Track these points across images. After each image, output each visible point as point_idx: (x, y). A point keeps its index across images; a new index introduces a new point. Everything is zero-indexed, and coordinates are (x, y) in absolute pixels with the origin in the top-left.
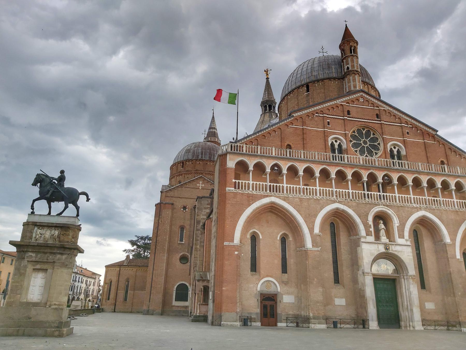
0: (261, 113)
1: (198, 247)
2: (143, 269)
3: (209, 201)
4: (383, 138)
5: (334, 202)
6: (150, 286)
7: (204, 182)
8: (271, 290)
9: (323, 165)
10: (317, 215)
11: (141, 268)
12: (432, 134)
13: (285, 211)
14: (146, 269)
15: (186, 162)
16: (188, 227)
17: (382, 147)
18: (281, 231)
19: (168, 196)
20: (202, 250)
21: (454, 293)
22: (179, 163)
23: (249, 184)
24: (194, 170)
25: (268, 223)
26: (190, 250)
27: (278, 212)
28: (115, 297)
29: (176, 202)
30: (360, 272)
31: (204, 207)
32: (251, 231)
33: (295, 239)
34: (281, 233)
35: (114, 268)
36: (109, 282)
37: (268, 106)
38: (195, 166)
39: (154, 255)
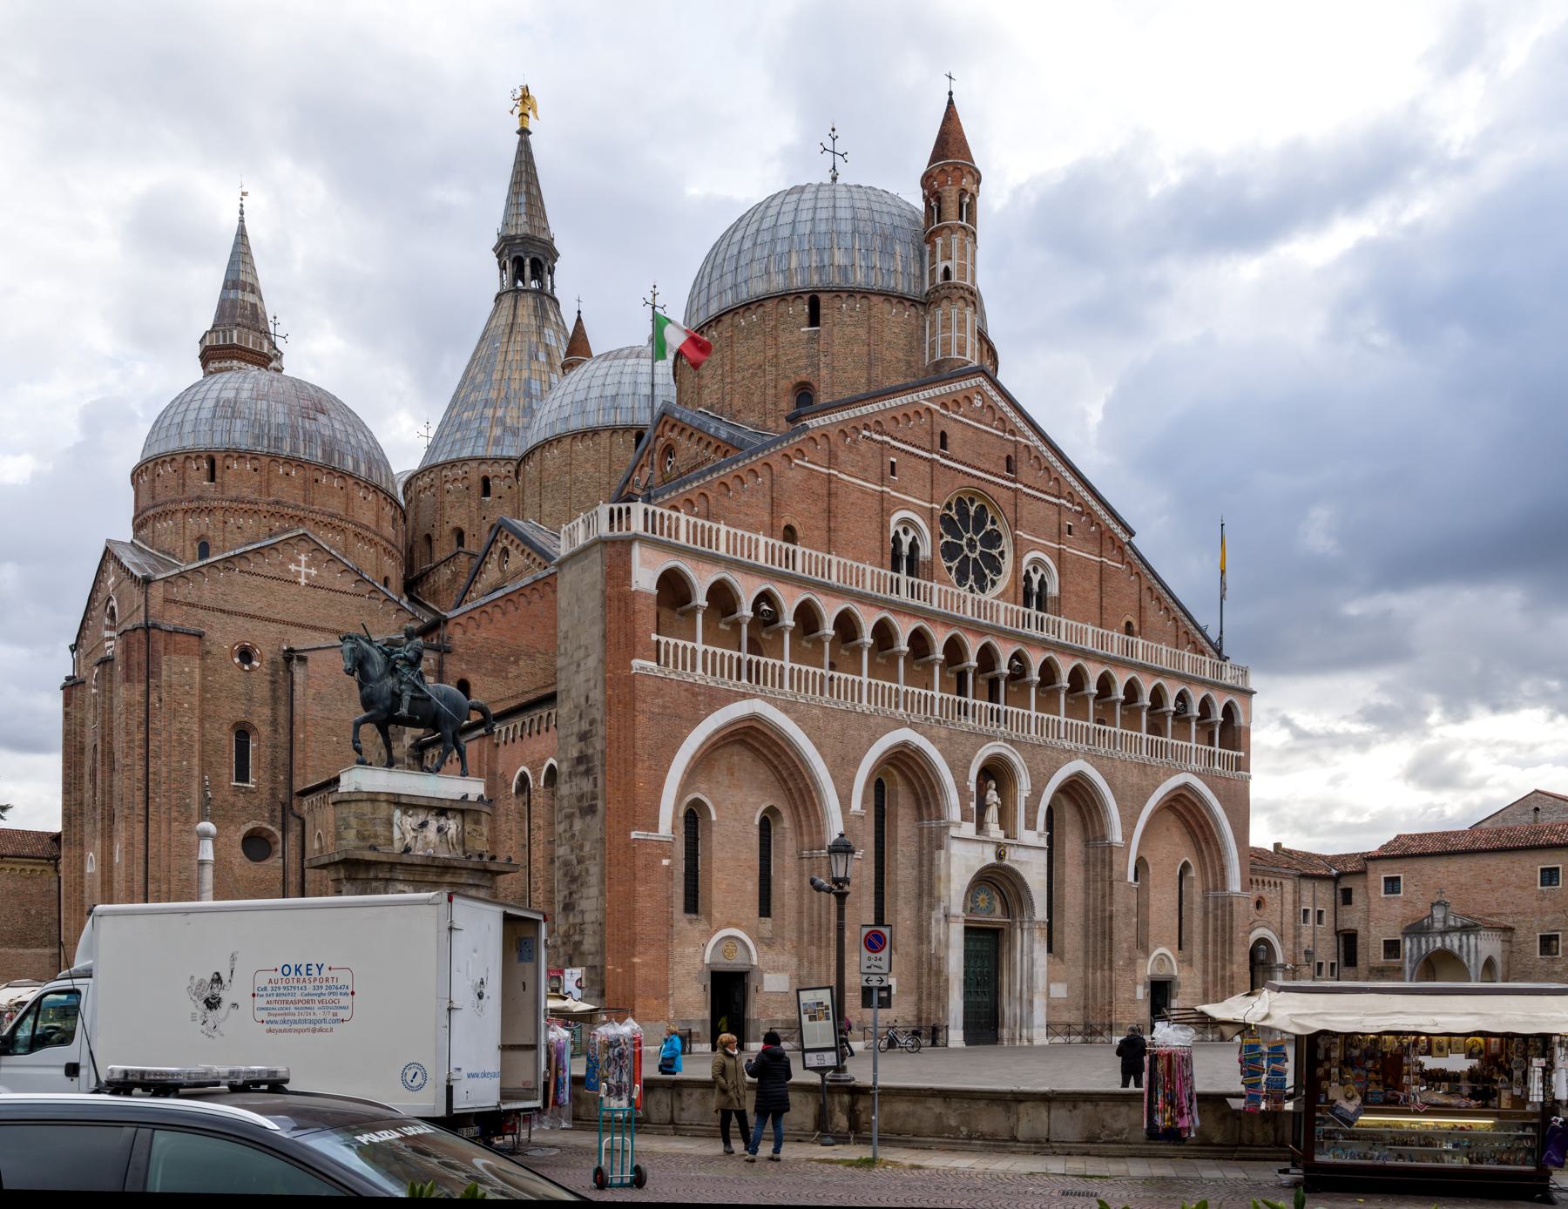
0: (497, 289)
4: (1015, 538)
5: (901, 724)
8: (736, 962)
9: (882, 608)
10: (860, 761)
12: (1120, 540)
13: (783, 745)
14: (31, 867)
17: (1007, 565)
18: (763, 801)
21: (1111, 962)
22: (188, 457)
23: (694, 650)
24: (265, 498)
25: (732, 774)
26: (279, 814)
27: (762, 743)
29: (211, 627)
30: (938, 914)
32: (689, 798)
33: (798, 825)
34: (763, 807)
38: (269, 485)
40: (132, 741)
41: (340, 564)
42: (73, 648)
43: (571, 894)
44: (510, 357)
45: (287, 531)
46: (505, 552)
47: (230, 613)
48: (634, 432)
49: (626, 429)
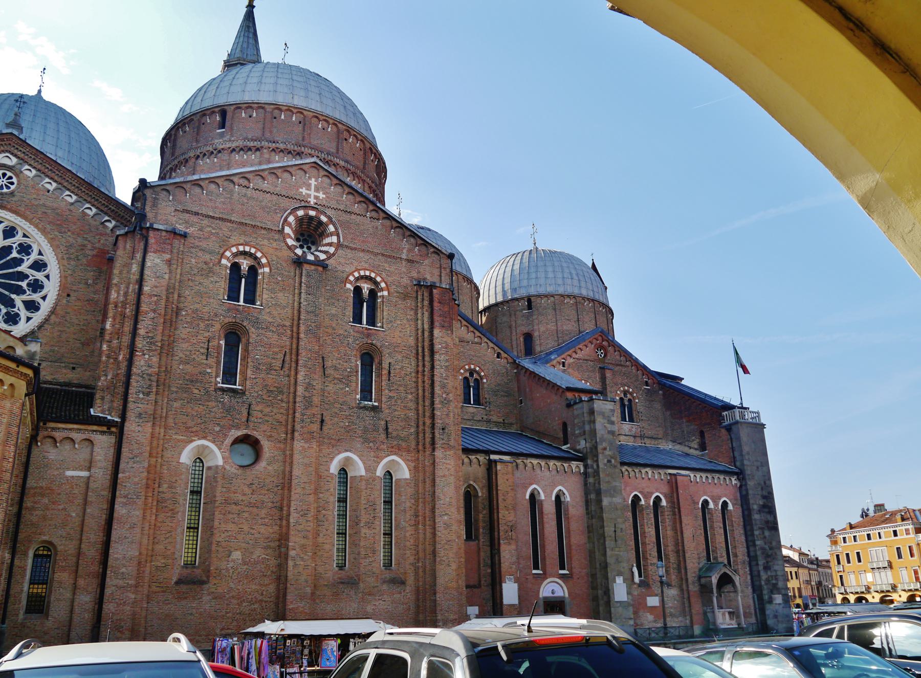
43: (767, 562)
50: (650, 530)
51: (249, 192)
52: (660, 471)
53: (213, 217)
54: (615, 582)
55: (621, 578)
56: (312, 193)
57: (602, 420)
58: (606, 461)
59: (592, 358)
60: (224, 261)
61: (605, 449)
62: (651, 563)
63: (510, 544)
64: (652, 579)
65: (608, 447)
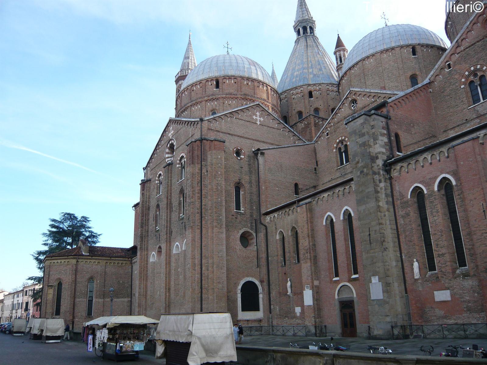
1: (382, 204)
2: (116, 262)
3: (384, 123)
6: (200, 287)
7: (262, 114)
11: (113, 260)
15: (223, 79)
16: (247, 186)
19: (212, 130)
20: (392, 210)
28: (72, 310)
31: (379, 132)
35: (64, 260)
36: (56, 284)
37: (308, 27)
39: (199, 230)
40: (194, 191)
41: (271, 116)
42: (144, 169)
44: (309, 54)
45: (246, 104)
46: (354, 101)
47: (232, 135)
48: (411, 47)
49: (408, 46)
50: (435, 218)
51: (160, 149)
52: (442, 149)
53: (155, 167)
54: (371, 282)
55: (377, 278)
56: (171, 133)
57: (354, 139)
58: (359, 173)
59: (480, 38)
60: (157, 182)
61: (358, 162)
62: (439, 254)
63: (306, 262)
64: (441, 271)
65: (360, 162)
